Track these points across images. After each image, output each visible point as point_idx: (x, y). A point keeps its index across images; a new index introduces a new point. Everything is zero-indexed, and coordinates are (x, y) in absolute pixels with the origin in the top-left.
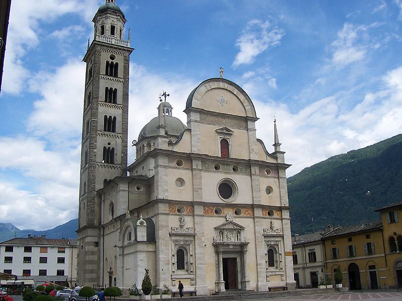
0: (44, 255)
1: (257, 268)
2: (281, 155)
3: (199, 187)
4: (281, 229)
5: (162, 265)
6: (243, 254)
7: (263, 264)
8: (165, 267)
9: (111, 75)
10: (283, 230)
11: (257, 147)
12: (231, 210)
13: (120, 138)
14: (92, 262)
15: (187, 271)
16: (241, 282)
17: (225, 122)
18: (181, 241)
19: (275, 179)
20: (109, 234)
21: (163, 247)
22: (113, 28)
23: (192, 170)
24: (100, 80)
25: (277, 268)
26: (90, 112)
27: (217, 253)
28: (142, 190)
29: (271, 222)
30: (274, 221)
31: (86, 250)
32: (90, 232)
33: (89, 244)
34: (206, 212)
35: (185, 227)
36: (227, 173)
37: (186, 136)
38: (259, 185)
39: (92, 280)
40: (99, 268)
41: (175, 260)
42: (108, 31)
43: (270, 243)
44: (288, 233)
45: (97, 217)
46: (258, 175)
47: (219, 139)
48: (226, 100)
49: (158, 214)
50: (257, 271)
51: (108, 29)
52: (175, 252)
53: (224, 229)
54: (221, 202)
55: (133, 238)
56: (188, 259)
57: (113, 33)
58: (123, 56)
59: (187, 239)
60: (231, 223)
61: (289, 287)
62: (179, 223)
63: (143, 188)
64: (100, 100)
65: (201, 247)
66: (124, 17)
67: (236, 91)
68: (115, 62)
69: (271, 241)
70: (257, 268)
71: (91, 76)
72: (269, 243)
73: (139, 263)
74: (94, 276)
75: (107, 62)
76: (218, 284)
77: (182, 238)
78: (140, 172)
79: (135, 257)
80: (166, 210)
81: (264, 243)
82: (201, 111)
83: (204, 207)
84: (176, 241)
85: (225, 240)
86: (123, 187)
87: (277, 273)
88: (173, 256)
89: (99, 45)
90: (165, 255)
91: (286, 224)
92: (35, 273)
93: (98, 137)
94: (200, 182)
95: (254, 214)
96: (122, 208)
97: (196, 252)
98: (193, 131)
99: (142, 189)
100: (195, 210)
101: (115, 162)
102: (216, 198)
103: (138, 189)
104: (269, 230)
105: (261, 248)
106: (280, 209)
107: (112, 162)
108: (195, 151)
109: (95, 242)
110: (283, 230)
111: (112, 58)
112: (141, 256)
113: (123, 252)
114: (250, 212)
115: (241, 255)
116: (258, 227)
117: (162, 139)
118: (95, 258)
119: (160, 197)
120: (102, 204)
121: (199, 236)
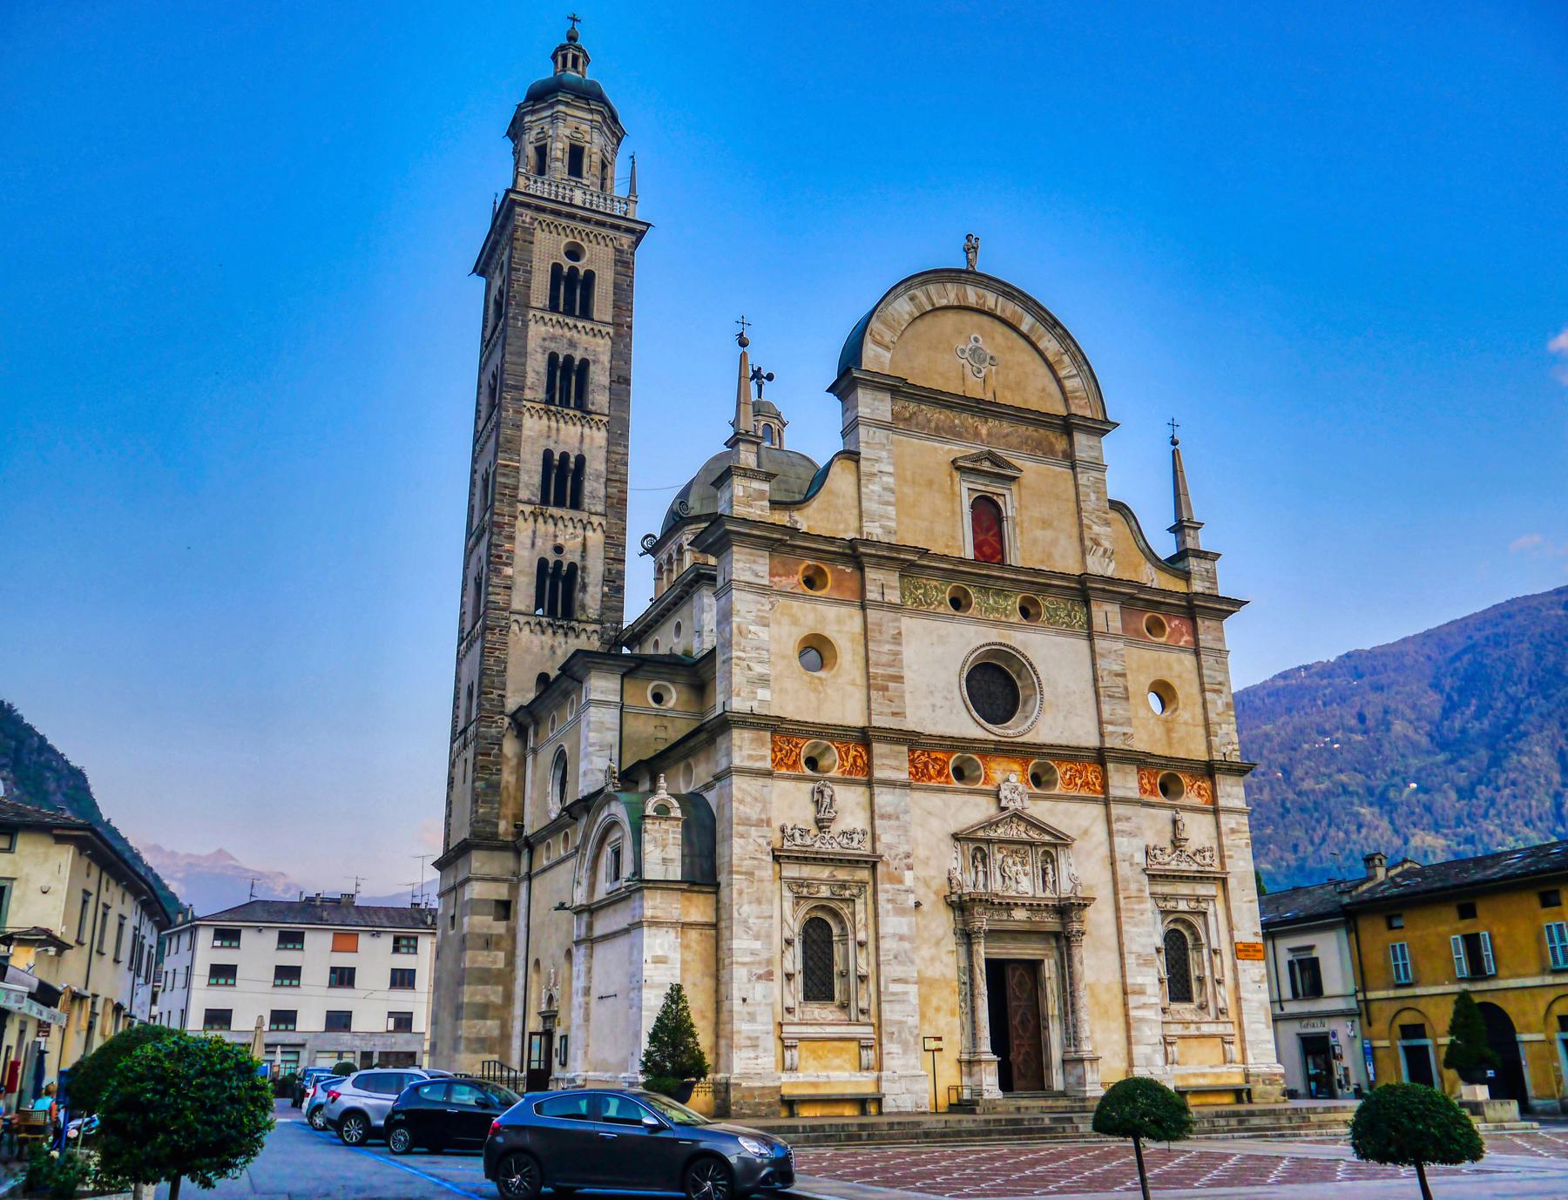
0: (343, 960)
1: (1125, 1004)
2: (1207, 565)
3: (891, 671)
4: (1216, 853)
5: (740, 981)
6: (1069, 948)
7: (1149, 990)
8: (759, 991)
9: (569, 312)
10: (1222, 857)
11: (1108, 532)
12: (1016, 767)
13: (599, 530)
14: (485, 977)
15: (844, 1007)
16: (1064, 1062)
17: (989, 435)
18: (822, 882)
19: (1182, 655)
20: (551, 867)
21: (746, 909)
22: (576, 155)
23: (863, 607)
24: (532, 324)
25: (1202, 1007)
26: (493, 440)
27: (967, 937)
28: (671, 704)
29: (1175, 822)
30: (1185, 817)
31: (466, 929)
32: (479, 862)
33: (476, 906)
34: (919, 773)
35: (836, 828)
36: (996, 624)
37: (841, 480)
39: (482, 1044)
40: (508, 997)
41: (794, 960)
42: (559, 164)
43: (1172, 904)
44: (1241, 865)
45: (509, 810)
46: (1116, 637)
47: (965, 491)
48: (989, 352)
49: (728, 772)
50: (1127, 1015)
51: (559, 154)
52: (796, 927)
53: (989, 841)
54: (978, 733)
55: (627, 870)
56: (850, 959)
57: (575, 167)
58: (610, 250)
59: (842, 875)
60: (1018, 816)
61: (1259, 1088)
62: (812, 808)
63: (674, 696)
64: (528, 394)
65: (901, 911)
66: (615, 119)
67: (1027, 323)
68: (582, 266)
69: (1175, 897)
70: (1125, 1004)
71: (499, 314)
72: (1170, 905)
73: (649, 971)
74: (491, 1026)
76: (969, 1064)
77: (824, 873)
78: (666, 642)
79: (632, 947)
80: (763, 758)
81: (1149, 905)
82: (896, 388)
83: (911, 751)
84: (800, 883)
85: (996, 885)
86: (602, 686)
87: (1206, 1029)
88: (789, 942)
89: (528, 206)
90: (757, 937)
91: (1233, 831)
92: (311, 1021)
93: (520, 522)
94: (897, 654)
95: (1105, 787)
96: (592, 771)
97: (881, 932)
99: (673, 698)
100: (876, 761)
101: (579, 614)
102: (964, 724)
103: (658, 698)
104: (1169, 850)
105: (1136, 925)
106: (1209, 770)
107: (568, 613)
108: (874, 530)
109: (498, 902)
110: (1222, 857)
111: (574, 253)
112: (658, 941)
113: (590, 927)
114: (1091, 778)
115: (1059, 948)
116: (1125, 840)
117: (746, 482)
118: (498, 959)
119: (739, 705)
120: (530, 759)
121: (895, 863)
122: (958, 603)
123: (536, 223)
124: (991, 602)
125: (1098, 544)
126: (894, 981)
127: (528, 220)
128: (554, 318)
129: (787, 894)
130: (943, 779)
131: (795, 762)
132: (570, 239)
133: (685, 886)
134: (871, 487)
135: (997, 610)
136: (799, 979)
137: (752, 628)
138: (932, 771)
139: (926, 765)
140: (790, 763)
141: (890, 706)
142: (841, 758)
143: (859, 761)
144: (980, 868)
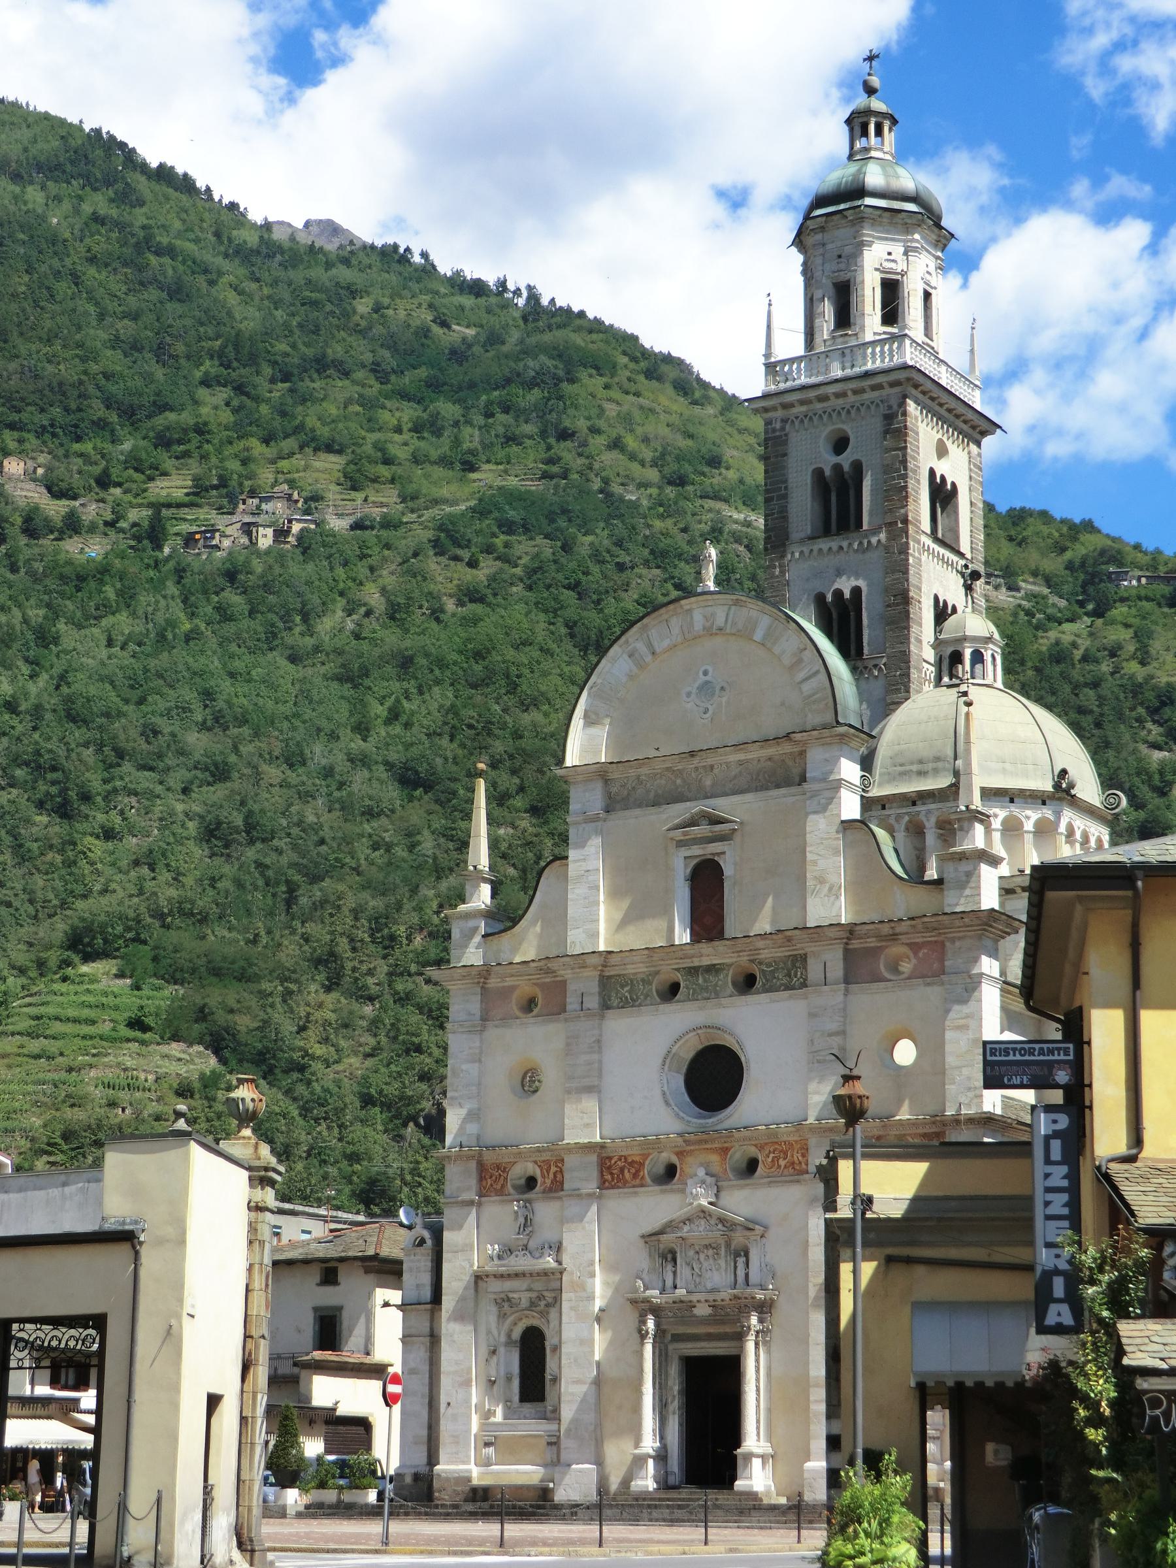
12: (714, 1158)
38: (843, 1033)
59: (538, 1285)
60: (703, 1213)
75: (819, 474)
98: (575, 861)
111: (841, 444)
114: (797, 1157)
122: (672, 991)
123: (787, 427)
124: (701, 981)
125: (821, 881)
126: (574, 1382)
127: (778, 426)
128: (816, 548)
129: (494, 1309)
130: (638, 1182)
131: (503, 1186)
132: (830, 428)
133: (429, 1306)
134: (577, 891)
135: (706, 989)
136: (516, 1383)
137: (464, 1067)
138: (627, 1175)
139: (622, 1170)
140: (499, 1187)
141: (582, 1118)
142: (543, 1176)
143: (559, 1176)
144: (669, 1267)
